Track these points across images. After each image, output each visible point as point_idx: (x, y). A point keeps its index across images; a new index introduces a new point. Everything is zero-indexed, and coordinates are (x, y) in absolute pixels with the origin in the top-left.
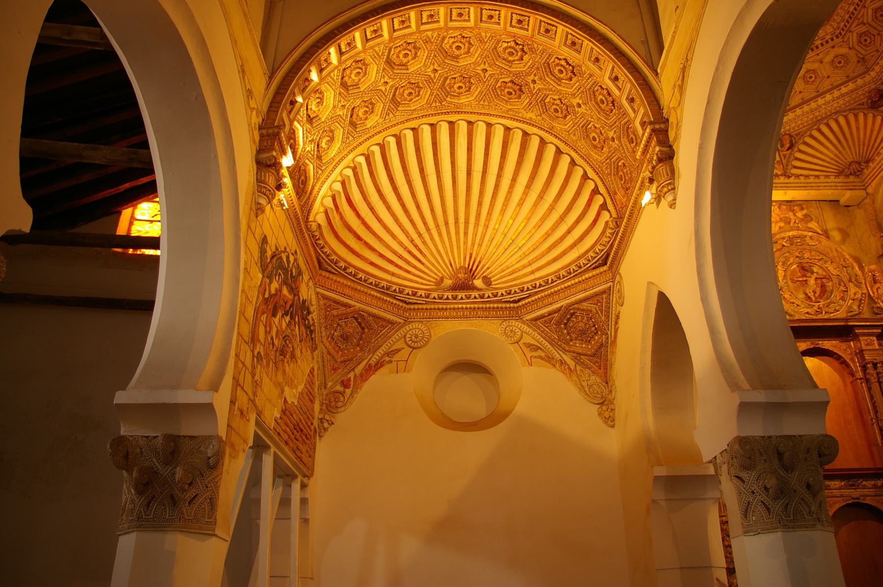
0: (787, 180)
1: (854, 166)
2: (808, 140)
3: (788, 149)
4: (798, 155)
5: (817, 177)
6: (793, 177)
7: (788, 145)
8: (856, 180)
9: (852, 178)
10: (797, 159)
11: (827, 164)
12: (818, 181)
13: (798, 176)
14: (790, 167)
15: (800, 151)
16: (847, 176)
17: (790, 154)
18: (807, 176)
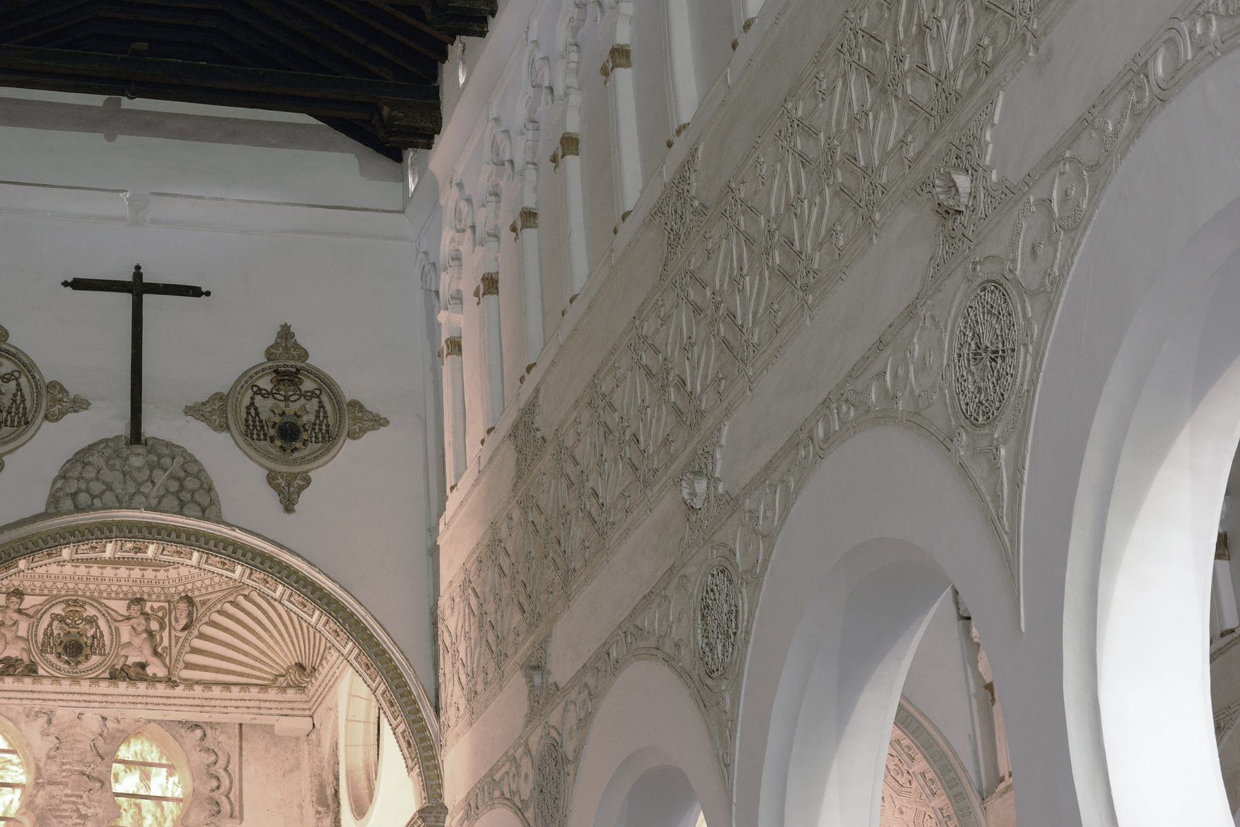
0: (170, 692)
1: (294, 676)
2: (217, 618)
3: (184, 629)
4: (198, 643)
5: (227, 685)
6: (181, 687)
7: (183, 622)
8: (299, 697)
9: (291, 694)
10: (194, 651)
11: (251, 662)
12: (226, 695)
13: (190, 684)
14: (181, 665)
15: (202, 636)
16: (283, 690)
17: (186, 639)
18: (207, 685)
